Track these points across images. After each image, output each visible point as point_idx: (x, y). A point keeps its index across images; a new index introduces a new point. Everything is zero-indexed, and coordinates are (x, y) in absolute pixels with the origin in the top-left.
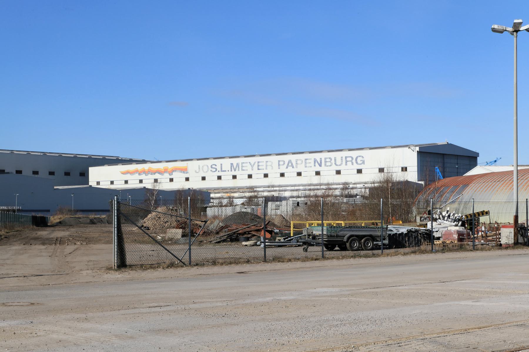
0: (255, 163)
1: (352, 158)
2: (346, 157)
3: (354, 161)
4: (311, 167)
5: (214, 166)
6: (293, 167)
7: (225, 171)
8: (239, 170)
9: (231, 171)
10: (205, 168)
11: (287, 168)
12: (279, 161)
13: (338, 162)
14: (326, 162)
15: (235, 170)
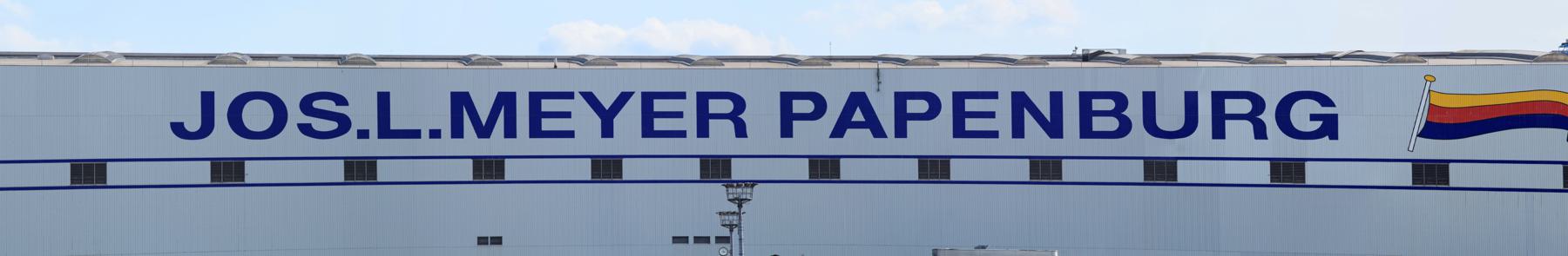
0: (624, 98)
1: (1258, 103)
2: (1219, 98)
3: (1268, 117)
4: (995, 134)
5: (317, 104)
6: (879, 132)
7: (415, 134)
8: (510, 132)
9: (457, 132)
10: (258, 116)
11: (838, 132)
12: (787, 98)
13: (1170, 115)
14: (1086, 114)
15: (484, 131)
